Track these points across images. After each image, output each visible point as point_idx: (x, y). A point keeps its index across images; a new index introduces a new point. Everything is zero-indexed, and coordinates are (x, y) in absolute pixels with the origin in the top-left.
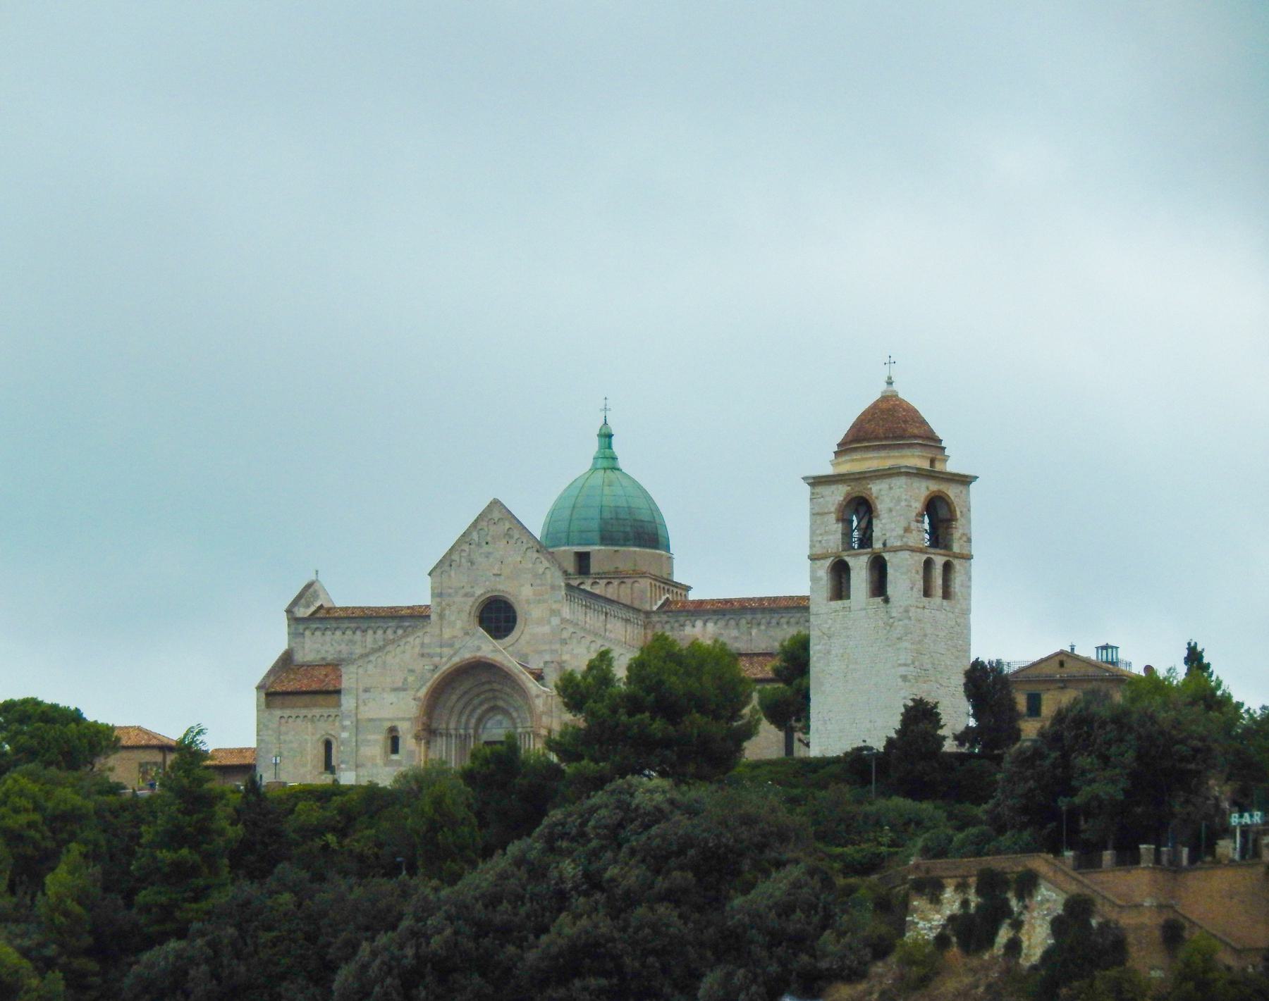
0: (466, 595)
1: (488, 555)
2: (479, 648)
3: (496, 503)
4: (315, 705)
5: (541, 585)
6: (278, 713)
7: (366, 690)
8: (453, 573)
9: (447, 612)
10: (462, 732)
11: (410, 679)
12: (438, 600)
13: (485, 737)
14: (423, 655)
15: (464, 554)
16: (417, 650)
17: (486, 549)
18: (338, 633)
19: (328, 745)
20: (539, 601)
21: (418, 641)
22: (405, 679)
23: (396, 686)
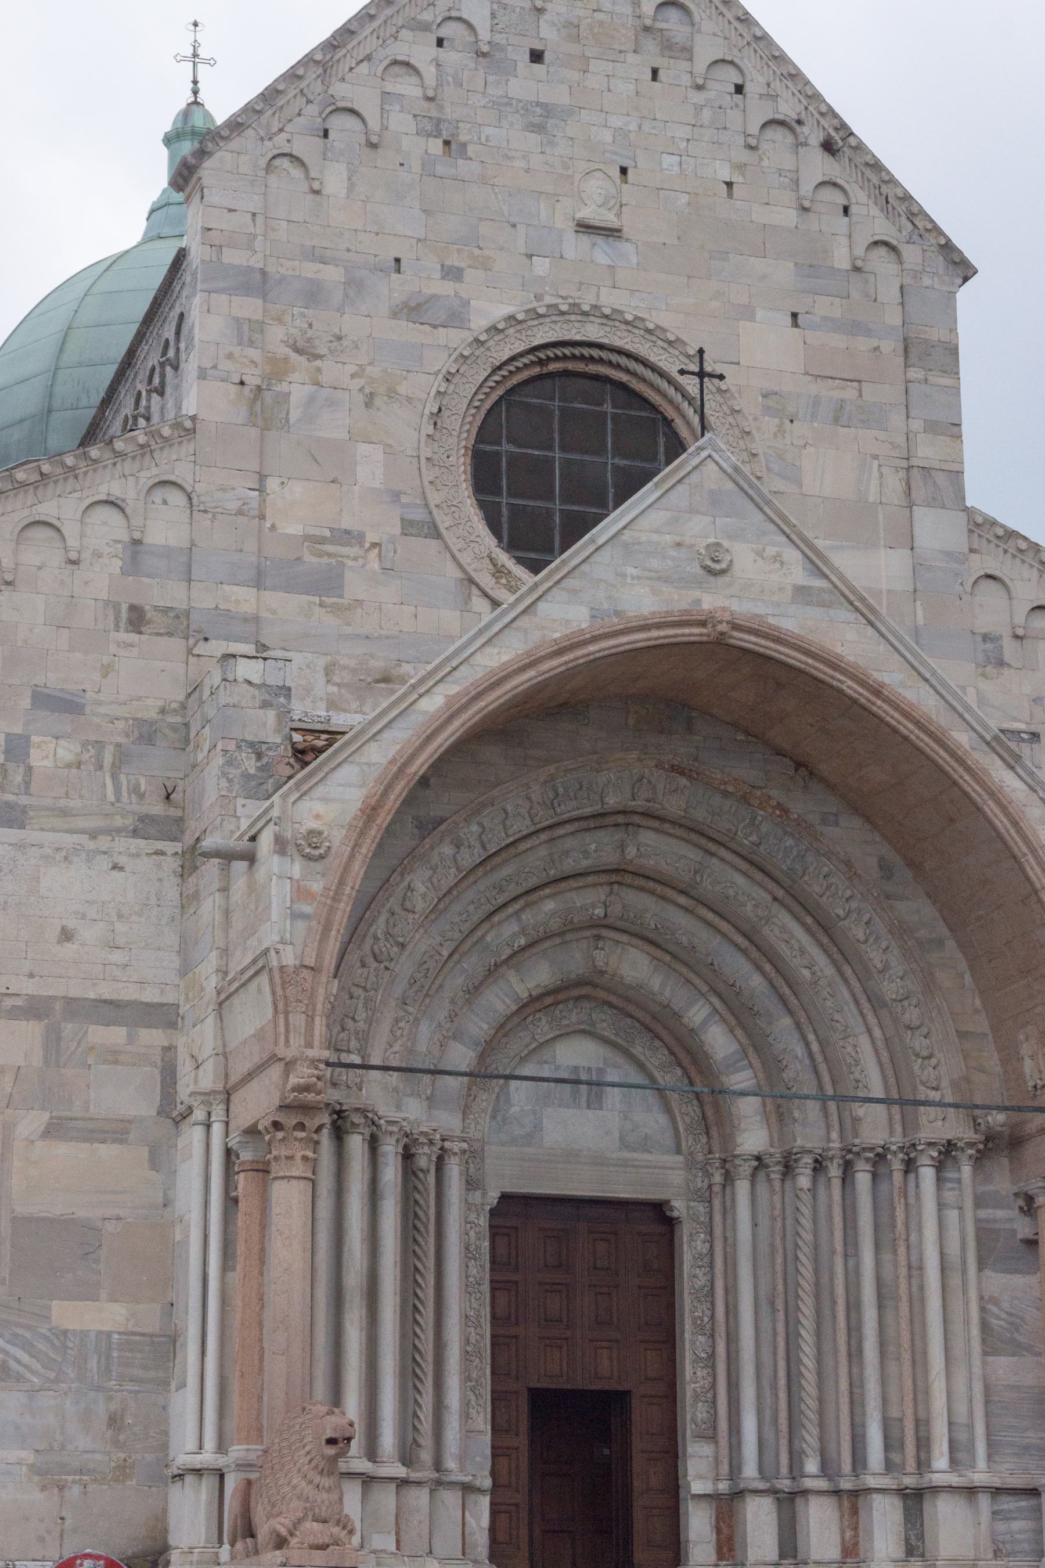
0: (413, 310)
1: (541, 119)
5: (855, 328)
9: (298, 390)
10: (413, 1112)
11: (51, 753)
12: (250, 307)
13: (505, 1176)
14: (137, 619)
15: (406, 87)
16: (102, 578)
20: (838, 416)
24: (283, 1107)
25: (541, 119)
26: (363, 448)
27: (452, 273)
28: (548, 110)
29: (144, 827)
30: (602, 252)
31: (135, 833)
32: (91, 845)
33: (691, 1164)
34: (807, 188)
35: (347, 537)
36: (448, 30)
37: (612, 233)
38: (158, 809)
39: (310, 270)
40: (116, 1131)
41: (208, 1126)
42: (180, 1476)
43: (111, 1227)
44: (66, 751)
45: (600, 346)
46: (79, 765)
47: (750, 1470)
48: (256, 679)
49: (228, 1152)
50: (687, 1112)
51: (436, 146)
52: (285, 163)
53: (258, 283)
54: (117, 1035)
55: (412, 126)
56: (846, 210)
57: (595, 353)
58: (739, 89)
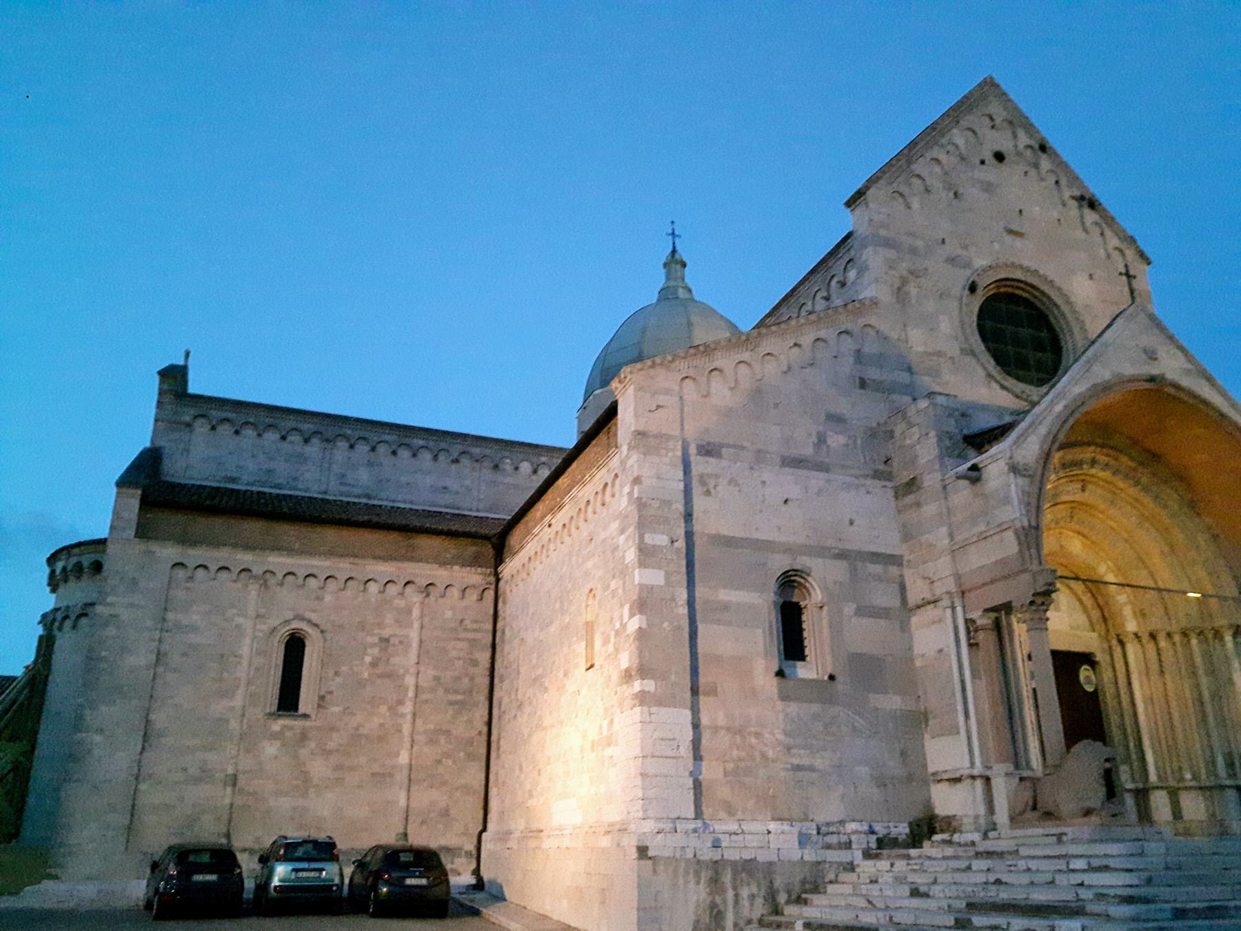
0: (952, 260)
2: (1152, 356)
3: (989, 87)
4: (276, 548)
6: (168, 552)
7: (708, 450)
8: (916, 205)
9: (913, 290)
14: (863, 384)
15: (937, 169)
16: (847, 365)
17: (981, 174)
18: (271, 436)
19: (295, 648)
21: (848, 344)
22: (821, 440)
23: (793, 452)
24: (1034, 595)
25: (988, 187)
26: (941, 317)
27: (965, 247)
28: (990, 184)
29: (877, 475)
30: (1018, 243)
31: (874, 477)
32: (857, 482)
33: (1100, 635)
34: (1088, 224)
35: (939, 354)
36: (950, 148)
37: (1019, 235)
38: (882, 467)
39: (910, 240)
40: (883, 613)
41: (953, 608)
42: (958, 780)
43: (890, 659)
44: (842, 439)
45: (1021, 281)
46: (847, 445)
47: (1153, 778)
48: (945, 404)
49: (966, 621)
50: (1096, 614)
51: (951, 195)
52: (896, 195)
53: (888, 243)
54: (877, 569)
55: (941, 186)
56: (1102, 234)
57: (1016, 284)
58: (1057, 182)
